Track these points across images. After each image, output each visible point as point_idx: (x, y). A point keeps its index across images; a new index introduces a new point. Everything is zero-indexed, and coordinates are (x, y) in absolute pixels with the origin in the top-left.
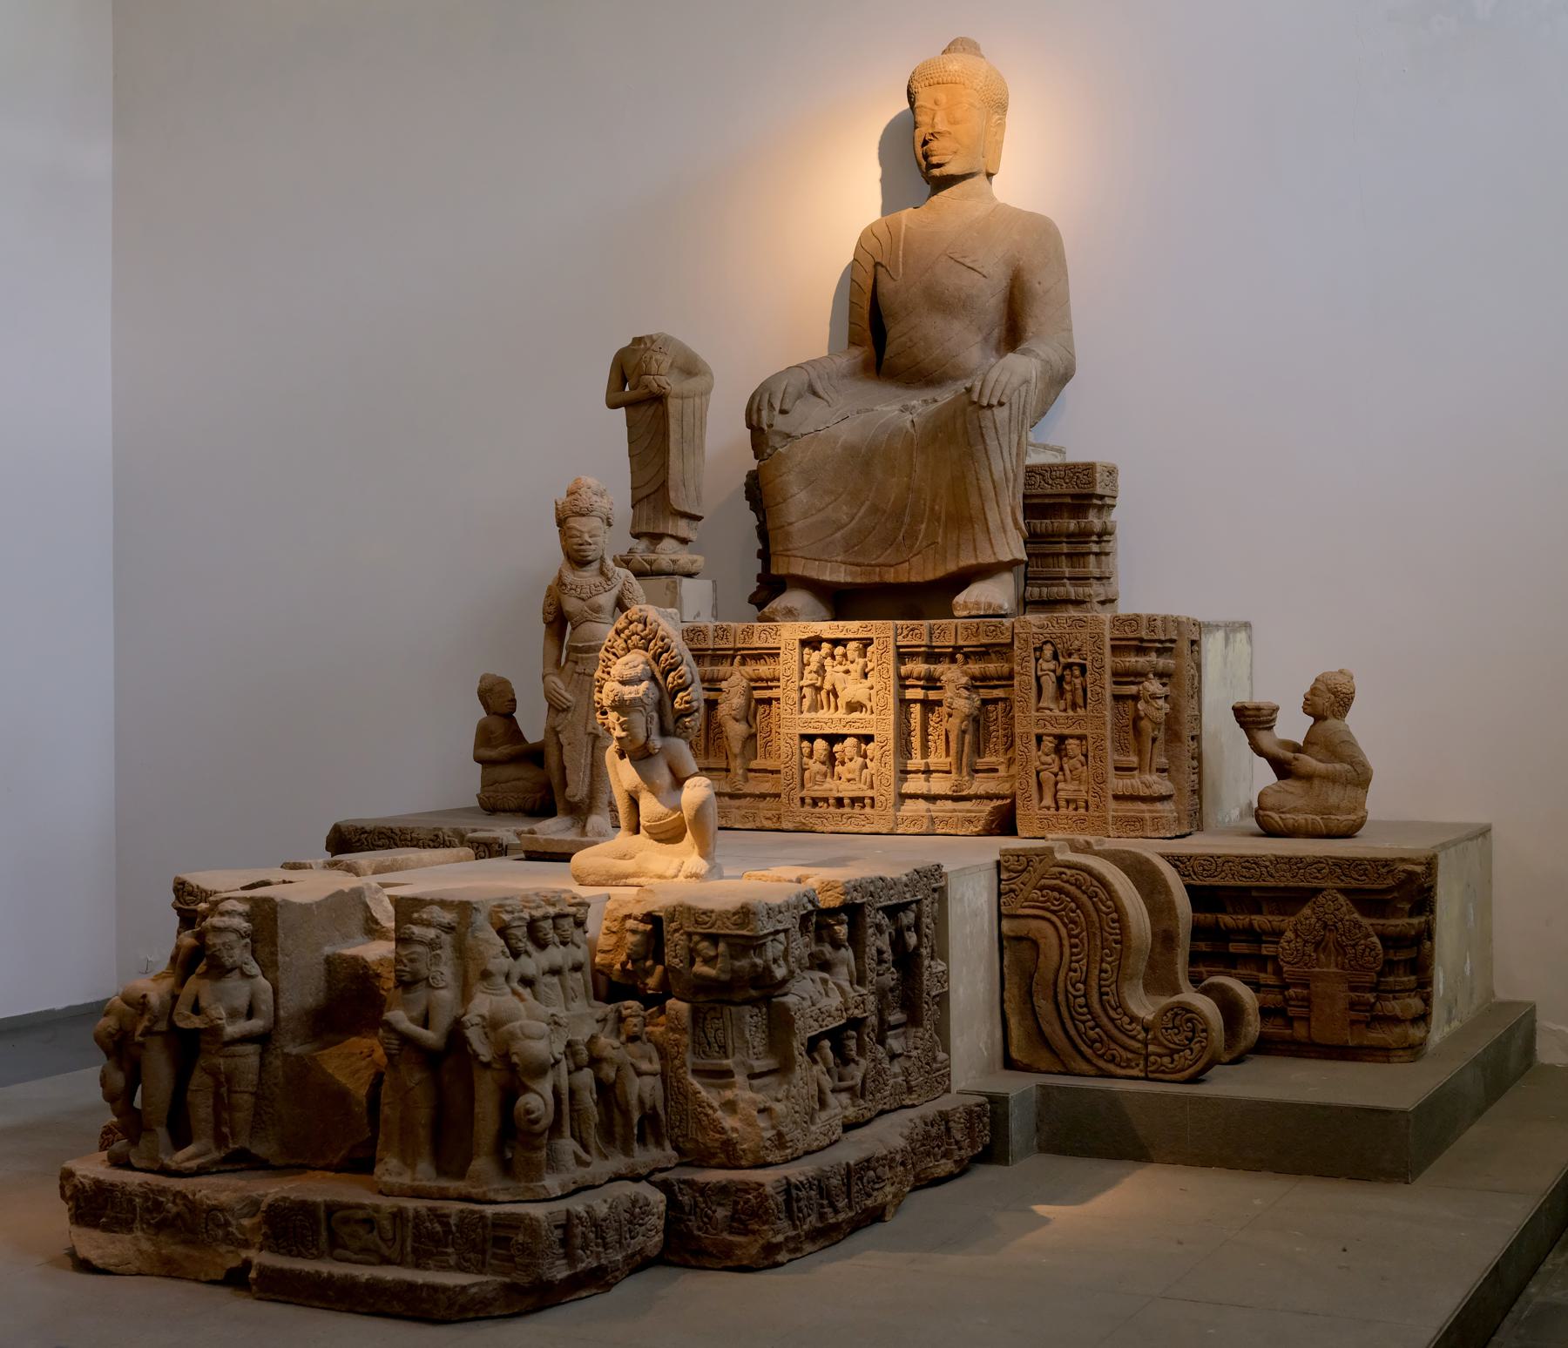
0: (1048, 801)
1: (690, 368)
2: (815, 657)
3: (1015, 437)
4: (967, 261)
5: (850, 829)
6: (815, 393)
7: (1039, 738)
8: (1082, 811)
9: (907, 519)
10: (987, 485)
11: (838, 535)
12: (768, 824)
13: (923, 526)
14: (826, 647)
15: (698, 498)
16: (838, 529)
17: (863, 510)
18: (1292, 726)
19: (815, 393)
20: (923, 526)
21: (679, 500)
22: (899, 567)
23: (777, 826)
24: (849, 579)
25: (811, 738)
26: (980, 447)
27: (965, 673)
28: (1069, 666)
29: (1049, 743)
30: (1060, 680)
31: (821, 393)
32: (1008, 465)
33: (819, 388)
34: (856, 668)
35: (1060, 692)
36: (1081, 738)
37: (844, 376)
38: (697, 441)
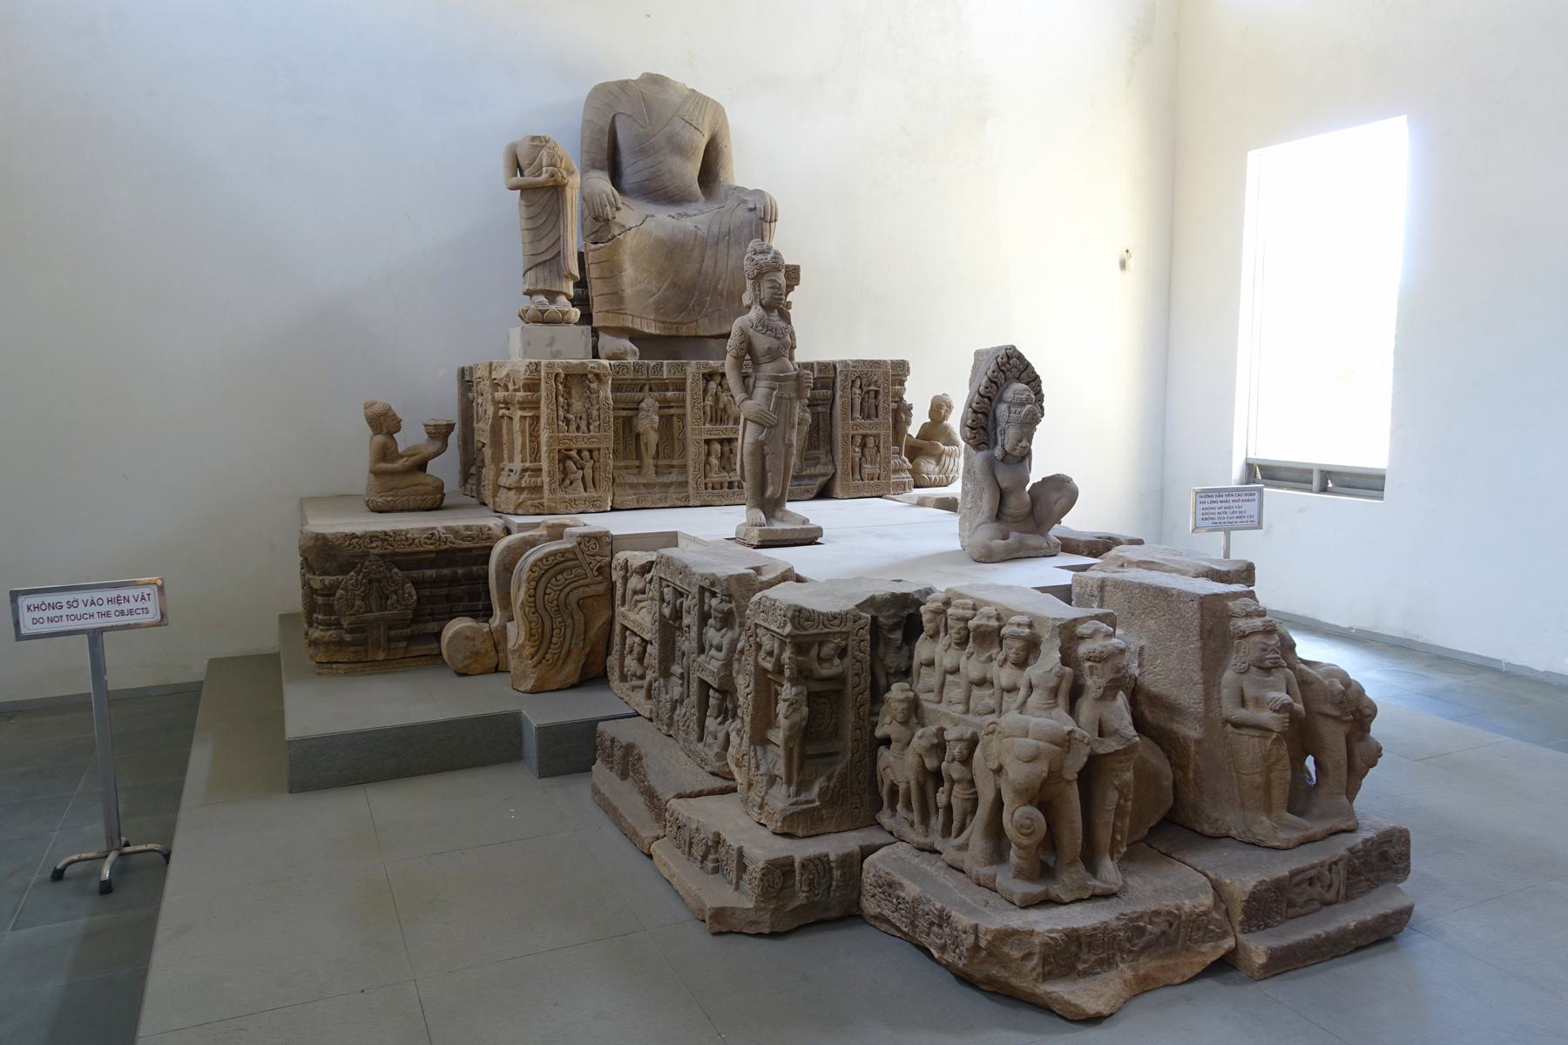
2: (713, 385)
25: (708, 442)
29: (859, 440)
36: (876, 436)
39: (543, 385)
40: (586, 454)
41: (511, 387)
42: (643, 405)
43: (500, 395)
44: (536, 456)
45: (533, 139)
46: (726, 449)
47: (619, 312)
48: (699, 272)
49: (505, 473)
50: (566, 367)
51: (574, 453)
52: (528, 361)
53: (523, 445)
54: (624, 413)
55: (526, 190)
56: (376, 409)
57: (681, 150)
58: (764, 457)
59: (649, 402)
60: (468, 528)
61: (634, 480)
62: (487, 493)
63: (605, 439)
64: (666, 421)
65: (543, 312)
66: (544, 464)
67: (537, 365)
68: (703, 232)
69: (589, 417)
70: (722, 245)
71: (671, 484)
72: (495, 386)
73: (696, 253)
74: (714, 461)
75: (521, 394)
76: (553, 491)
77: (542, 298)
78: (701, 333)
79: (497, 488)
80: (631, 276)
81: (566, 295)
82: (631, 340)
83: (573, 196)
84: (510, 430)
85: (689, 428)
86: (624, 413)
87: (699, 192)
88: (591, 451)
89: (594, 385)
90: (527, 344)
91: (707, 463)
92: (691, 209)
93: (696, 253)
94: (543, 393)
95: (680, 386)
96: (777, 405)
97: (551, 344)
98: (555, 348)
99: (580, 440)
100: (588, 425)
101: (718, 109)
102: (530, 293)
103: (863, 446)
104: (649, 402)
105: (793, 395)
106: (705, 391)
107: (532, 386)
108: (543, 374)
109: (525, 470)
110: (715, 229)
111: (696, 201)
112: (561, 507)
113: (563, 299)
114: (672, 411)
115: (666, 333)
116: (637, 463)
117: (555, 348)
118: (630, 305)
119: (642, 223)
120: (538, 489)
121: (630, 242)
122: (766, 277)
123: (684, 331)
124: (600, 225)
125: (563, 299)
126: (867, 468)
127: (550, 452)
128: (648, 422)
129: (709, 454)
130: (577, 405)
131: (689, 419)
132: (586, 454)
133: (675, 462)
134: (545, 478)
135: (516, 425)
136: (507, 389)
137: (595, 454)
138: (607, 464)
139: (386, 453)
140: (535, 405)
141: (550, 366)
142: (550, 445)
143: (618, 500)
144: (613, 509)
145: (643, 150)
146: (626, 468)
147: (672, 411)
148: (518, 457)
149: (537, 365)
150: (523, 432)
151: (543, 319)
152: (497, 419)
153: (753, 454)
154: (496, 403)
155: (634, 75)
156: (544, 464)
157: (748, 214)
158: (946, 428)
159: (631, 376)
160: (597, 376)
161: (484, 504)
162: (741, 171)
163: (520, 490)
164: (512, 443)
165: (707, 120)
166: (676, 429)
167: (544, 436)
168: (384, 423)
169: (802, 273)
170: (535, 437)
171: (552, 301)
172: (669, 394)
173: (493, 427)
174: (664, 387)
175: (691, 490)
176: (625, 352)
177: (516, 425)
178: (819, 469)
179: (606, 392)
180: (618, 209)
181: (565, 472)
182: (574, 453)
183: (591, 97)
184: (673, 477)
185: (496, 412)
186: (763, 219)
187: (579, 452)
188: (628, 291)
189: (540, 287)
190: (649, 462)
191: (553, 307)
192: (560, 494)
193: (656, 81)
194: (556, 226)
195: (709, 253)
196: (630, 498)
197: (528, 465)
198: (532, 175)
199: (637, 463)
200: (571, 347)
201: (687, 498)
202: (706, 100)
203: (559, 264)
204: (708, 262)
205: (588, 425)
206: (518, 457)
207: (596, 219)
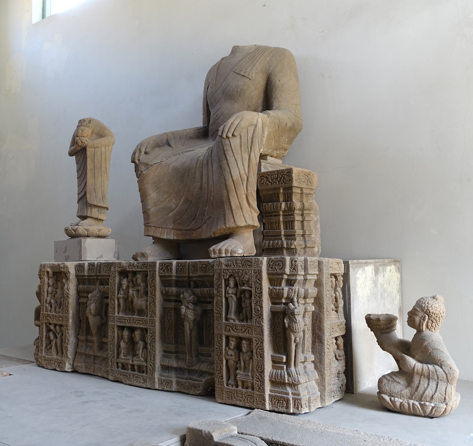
0: (231, 382)
1: (101, 133)
3: (246, 156)
4: (242, 73)
5: (137, 384)
6: (169, 145)
7: (227, 338)
8: (250, 390)
10: (230, 183)
11: (171, 214)
13: (207, 208)
15: (103, 197)
16: (171, 211)
18: (403, 332)
19: (169, 145)
21: (91, 199)
24: (175, 238)
25: (122, 328)
26: (225, 162)
27: (194, 293)
28: (244, 291)
29: (233, 343)
30: (239, 301)
31: (172, 145)
32: (242, 172)
33: (172, 143)
35: (239, 310)
37: (191, 138)
38: (103, 169)
40: (57, 327)
48: (201, 188)
50: (52, 267)
51: (52, 327)
91: (119, 346)
93: (197, 175)
97: (65, 252)
98: (67, 254)
103: (238, 348)
106: (120, 285)
117: (67, 254)
123: (195, 236)
126: (241, 374)
144: (75, 371)
178: (204, 367)
195: (205, 172)
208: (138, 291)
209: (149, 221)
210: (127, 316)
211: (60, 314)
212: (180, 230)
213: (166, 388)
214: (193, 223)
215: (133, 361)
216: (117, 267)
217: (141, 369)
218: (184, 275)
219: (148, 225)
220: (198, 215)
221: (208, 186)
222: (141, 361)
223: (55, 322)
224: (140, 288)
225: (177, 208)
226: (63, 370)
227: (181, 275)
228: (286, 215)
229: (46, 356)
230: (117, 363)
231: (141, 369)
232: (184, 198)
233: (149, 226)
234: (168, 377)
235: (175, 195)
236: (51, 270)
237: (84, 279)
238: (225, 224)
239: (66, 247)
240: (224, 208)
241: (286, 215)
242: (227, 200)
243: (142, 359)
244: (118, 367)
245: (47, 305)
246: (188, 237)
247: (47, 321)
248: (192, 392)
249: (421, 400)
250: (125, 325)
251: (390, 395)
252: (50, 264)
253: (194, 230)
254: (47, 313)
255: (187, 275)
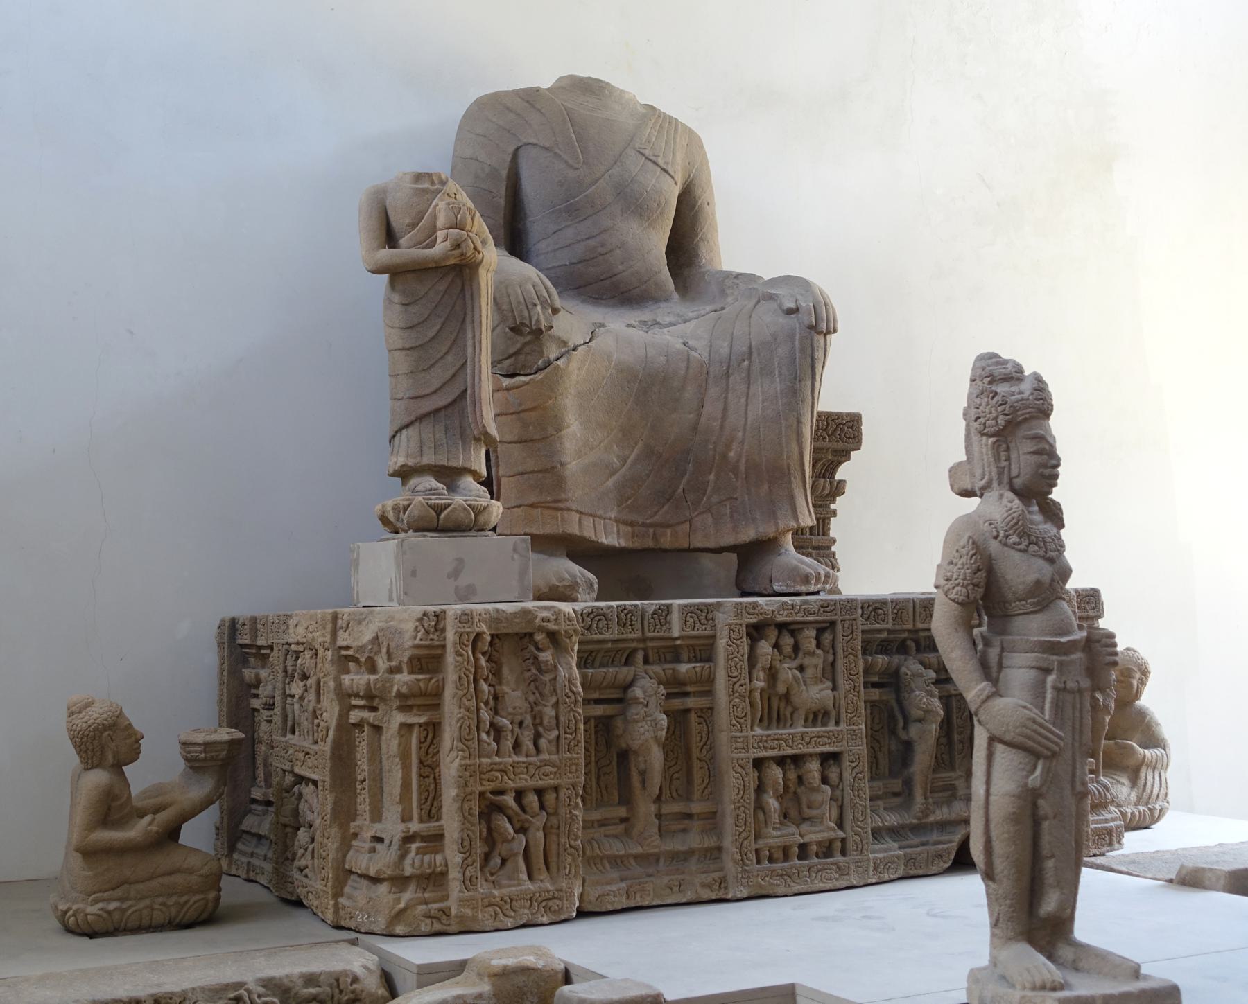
2: (765, 648)
5: (822, 886)
9: (690, 467)
12: (706, 894)
13: (712, 477)
14: (773, 634)
16: (613, 474)
17: (636, 451)
20: (712, 477)
22: (679, 528)
23: (720, 895)
24: (623, 543)
25: (758, 763)
26: (809, 383)
34: (817, 661)
39: (450, 658)
41: (382, 664)
42: (638, 692)
43: (357, 679)
44: (431, 811)
45: (418, 177)
46: (792, 776)
47: (556, 506)
48: (695, 428)
49: (363, 843)
50: (496, 619)
52: (418, 610)
53: (406, 785)
54: (599, 710)
55: (397, 274)
56: (95, 714)
57: (637, 205)
58: (1036, 822)
59: (647, 688)
60: (311, 979)
61: (617, 848)
62: (315, 886)
63: (566, 765)
64: (678, 719)
65: (439, 509)
66: (451, 824)
67: (440, 616)
68: (701, 351)
69: (537, 719)
70: (736, 379)
71: (691, 852)
72: (345, 660)
73: (690, 393)
74: (772, 803)
75: (404, 679)
76: (468, 883)
77: (431, 482)
78: (698, 542)
79: (344, 874)
80: (580, 440)
81: (475, 474)
82: (573, 557)
83: (486, 280)
84: (375, 753)
85: (723, 738)
86: (599, 710)
87: (671, 285)
88: (540, 792)
89: (546, 656)
90: (410, 574)
91: (759, 806)
92: (664, 312)
93: (690, 393)
94: (451, 676)
95: (704, 651)
96: (1057, 706)
97: (456, 574)
98: (464, 580)
99: (519, 770)
100: (537, 736)
101: (693, 140)
102: (404, 474)
104: (647, 688)
105: (1086, 683)
106: (752, 659)
107: (427, 661)
108: (450, 636)
109: (408, 839)
110: (725, 351)
111: (667, 300)
112: (484, 917)
113: (468, 482)
114: (691, 702)
115: (636, 544)
116: (622, 812)
117: (464, 580)
118: (577, 492)
119: (598, 342)
120: (434, 879)
121: (576, 373)
122: (1023, 431)
123: (667, 541)
124: (525, 344)
125: (468, 482)
127: (464, 798)
128: (647, 728)
129: (760, 789)
130: (515, 697)
131: (723, 716)
132: (532, 799)
133: (696, 808)
134: (452, 855)
135: (390, 743)
136: (373, 669)
137: (550, 797)
138: (573, 818)
139: (111, 808)
140: (430, 700)
141: (465, 618)
142: (463, 784)
143: (593, 893)
145: (573, 207)
146: (603, 823)
147: (691, 702)
148: (392, 812)
149: (440, 616)
150: (405, 756)
151: (439, 523)
152: (347, 730)
153: (1015, 819)
154: (344, 696)
155: (546, 81)
156: (451, 824)
157: (783, 320)
158: (1142, 714)
159: (613, 633)
160: (553, 636)
161: (298, 904)
162: (734, 247)
163: (400, 882)
164: (378, 778)
165: (679, 157)
166: (695, 739)
167: (451, 766)
168: (106, 743)
169: (865, 428)
170: (429, 768)
171: (452, 488)
172: (684, 668)
173: (337, 745)
174: (673, 653)
175: (731, 868)
176: (574, 586)
177: (390, 743)
179: (570, 670)
180: (555, 311)
181: (491, 839)
182: (509, 800)
183: (468, 116)
184: (695, 840)
185: (344, 715)
186: (813, 328)
187: (519, 795)
188: (573, 466)
189: (428, 459)
190: (646, 808)
191: (458, 499)
192: (483, 888)
193: (589, 88)
194: (457, 343)
195: (713, 391)
196: (615, 890)
197: (415, 826)
198: (417, 244)
199: (622, 812)
200: (499, 580)
201: (722, 883)
202: (673, 123)
203: (463, 414)
204: (711, 409)
205: (537, 736)
206: (392, 812)
207: (516, 330)
208: (801, 669)
209: (563, 496)
210: (784, 732)
211: (545, 756)
212: (632, 524)
213: (886, 877)
214: (666, 507)
215: (801, 836)
216: (745, 614)
217: (827, 850)
218: (905, 627)
219: (560, 505)
220: (680, 490)
221: (722, 427)
222: (830, 829)
223: (525, 781)
224: (807, 661)
225: (623, 469)
226: (563, 917)
227: (897, 627)
228: (820, 506)
229: (496, 892)
230: (757, 851)
231: (827, 850)
232: (641, 444)
233: (562, 509)
234: (886, 851)
235: (620, 435)
236: (489, 628)
237: (676, 647)
238: (796, 518)
239: (460, 561)
240: (790, 482)
241: (820, 506)
242: (798, 468)
243: (833, 825)
244: (758, 862)
245: (484, 736)
246: (650, 543)
247: (489, 786)
248: (935, 869)
249: (1147, 803)
250: (781, 753)
251: (1118, 806)
252: (487, 611)
253: (668, 526)
254: (485, 761)
255: (910, 626)
